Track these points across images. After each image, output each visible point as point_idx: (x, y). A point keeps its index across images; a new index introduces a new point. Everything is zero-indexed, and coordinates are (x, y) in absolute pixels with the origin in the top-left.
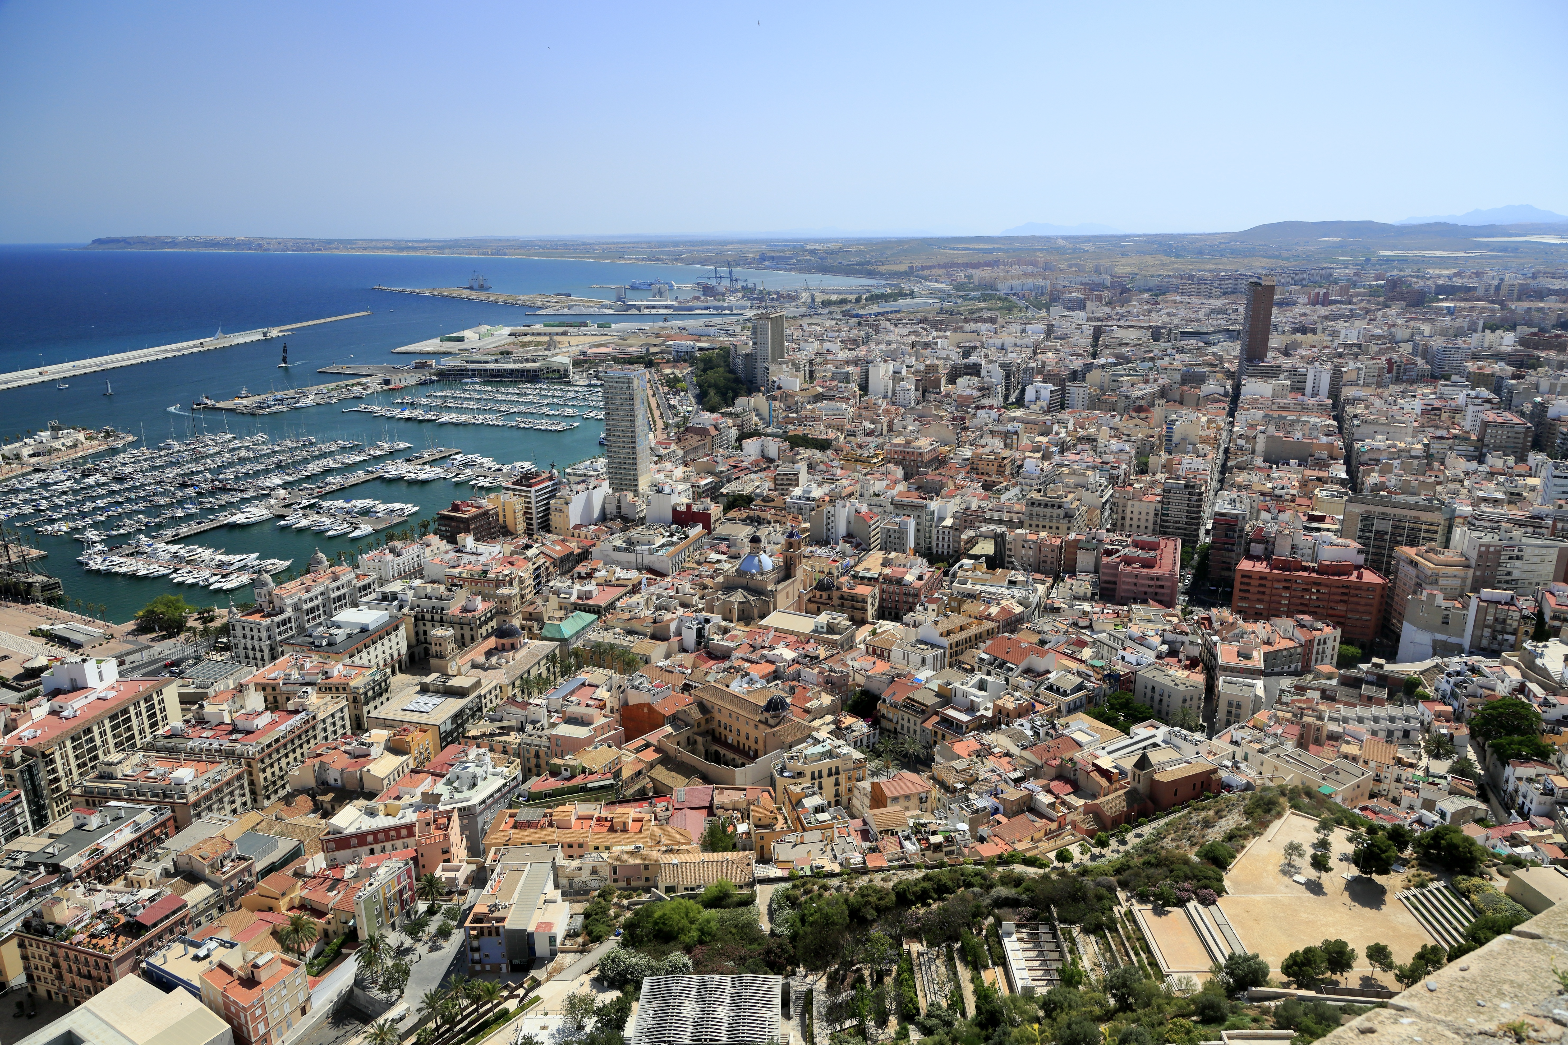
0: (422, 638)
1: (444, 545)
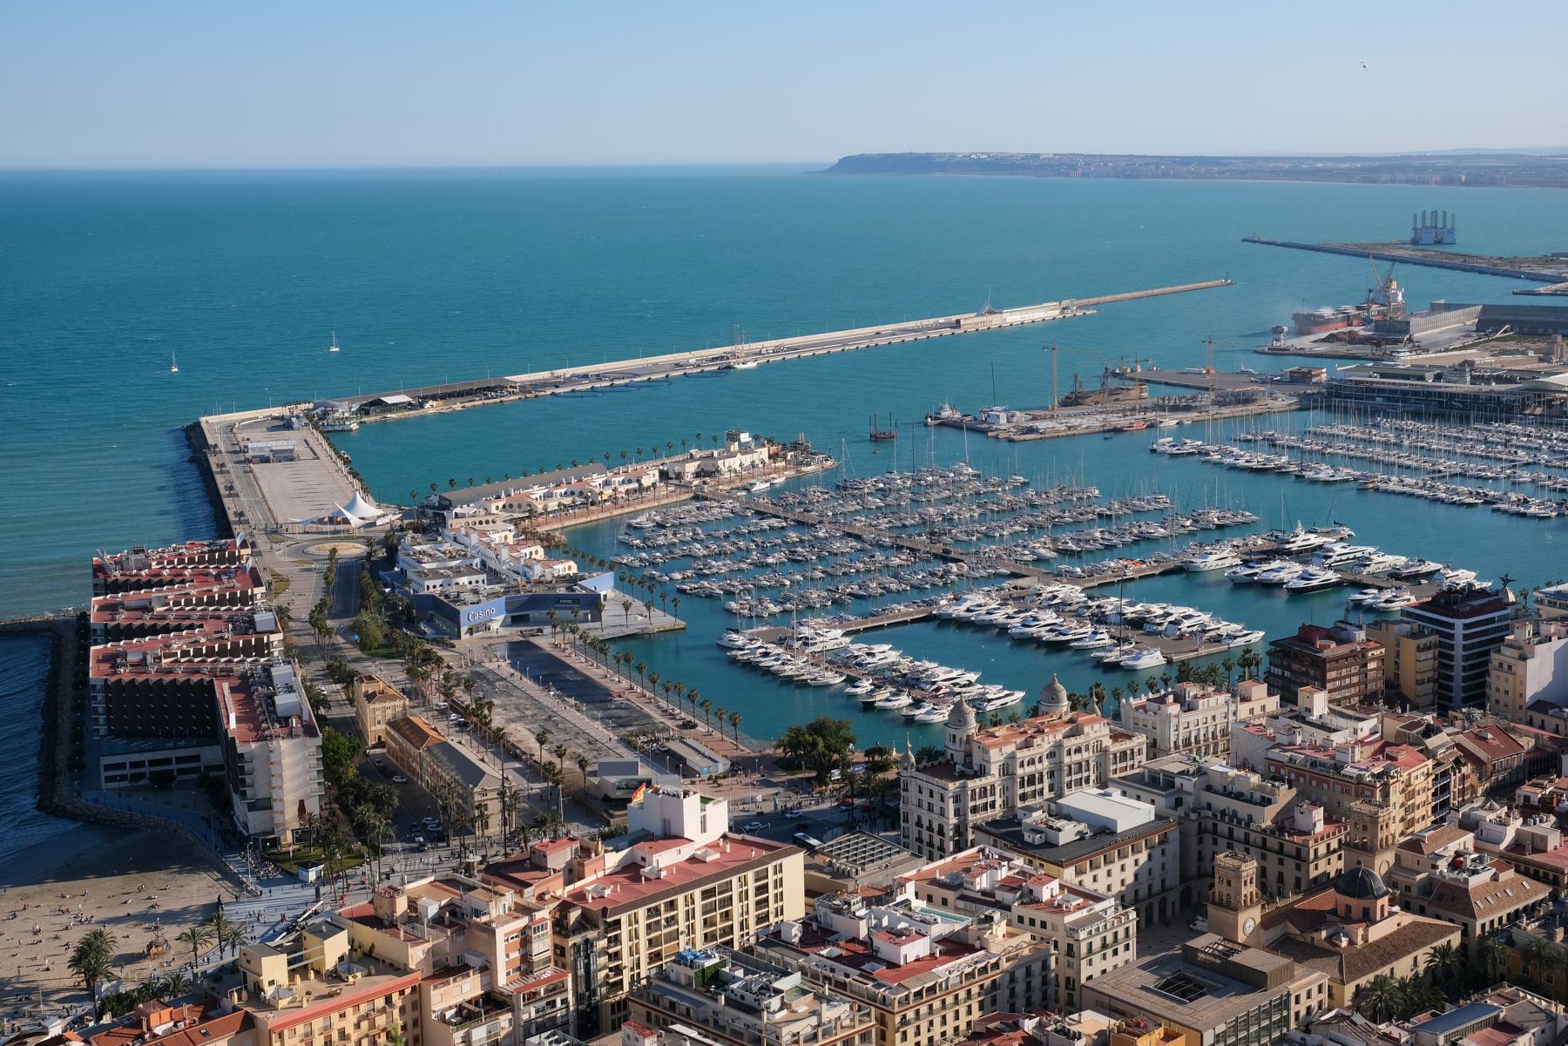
1: (1273, 703)
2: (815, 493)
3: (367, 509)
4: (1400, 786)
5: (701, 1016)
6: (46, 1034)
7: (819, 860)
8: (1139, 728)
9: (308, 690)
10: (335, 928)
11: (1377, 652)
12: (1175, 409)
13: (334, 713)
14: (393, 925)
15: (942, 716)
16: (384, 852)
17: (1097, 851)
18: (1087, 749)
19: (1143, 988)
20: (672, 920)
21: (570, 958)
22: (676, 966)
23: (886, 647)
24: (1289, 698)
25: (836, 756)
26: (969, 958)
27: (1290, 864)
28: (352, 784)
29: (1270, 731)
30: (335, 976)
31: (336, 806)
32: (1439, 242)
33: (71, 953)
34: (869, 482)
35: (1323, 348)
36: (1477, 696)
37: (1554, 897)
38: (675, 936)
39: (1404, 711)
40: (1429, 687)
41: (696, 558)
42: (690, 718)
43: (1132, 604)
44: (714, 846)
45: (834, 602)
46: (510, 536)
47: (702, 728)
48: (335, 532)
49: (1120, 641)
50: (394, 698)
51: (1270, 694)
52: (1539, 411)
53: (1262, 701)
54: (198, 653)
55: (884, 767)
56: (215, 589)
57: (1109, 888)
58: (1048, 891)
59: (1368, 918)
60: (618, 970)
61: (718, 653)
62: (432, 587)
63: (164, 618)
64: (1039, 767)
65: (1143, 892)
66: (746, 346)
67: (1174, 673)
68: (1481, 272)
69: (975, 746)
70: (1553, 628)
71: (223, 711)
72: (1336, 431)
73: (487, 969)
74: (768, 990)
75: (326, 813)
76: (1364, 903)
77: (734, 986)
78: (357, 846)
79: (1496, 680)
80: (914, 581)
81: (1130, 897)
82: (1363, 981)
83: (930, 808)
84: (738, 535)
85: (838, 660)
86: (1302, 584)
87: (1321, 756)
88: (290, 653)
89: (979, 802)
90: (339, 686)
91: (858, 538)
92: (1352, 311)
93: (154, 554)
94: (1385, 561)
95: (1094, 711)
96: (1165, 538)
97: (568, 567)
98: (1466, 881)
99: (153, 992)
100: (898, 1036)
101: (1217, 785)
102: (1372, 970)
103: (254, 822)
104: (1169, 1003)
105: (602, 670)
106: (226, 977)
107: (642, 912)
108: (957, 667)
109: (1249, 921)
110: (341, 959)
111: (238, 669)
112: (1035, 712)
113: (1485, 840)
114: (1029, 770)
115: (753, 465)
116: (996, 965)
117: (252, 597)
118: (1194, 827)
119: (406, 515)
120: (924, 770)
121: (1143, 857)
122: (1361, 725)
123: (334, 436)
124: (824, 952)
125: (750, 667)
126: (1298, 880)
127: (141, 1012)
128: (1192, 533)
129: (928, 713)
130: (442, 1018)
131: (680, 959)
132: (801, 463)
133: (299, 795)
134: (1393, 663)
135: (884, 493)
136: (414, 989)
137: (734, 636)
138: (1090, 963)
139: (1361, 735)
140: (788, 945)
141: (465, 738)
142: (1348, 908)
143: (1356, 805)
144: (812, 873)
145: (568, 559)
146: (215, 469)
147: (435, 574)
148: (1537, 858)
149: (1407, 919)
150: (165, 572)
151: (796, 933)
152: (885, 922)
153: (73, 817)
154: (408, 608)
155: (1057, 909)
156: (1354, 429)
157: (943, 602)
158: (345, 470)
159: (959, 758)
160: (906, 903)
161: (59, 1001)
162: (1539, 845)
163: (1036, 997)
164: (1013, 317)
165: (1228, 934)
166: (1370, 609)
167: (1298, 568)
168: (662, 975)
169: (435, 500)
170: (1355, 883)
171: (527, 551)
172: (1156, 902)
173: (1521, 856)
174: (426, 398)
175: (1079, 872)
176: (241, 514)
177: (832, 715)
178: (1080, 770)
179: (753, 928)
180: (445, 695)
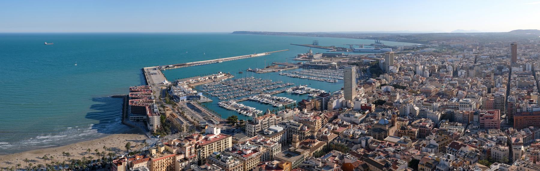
0: (291, 136)
2: (231, 81)
4: (317, 122)
5: (217, 163)
7: (234, 138)
8: (280, 116)
10: (163, 146)
12: (282, 68)
14: (171, 146)
15: (251, 115)
19: (283, 156)
20: (212, 147)
21: (197, 152)
22: (213, 155)
23: (242, 104)
24: (301, 110)
26: (257, 153)
27: (302, 135)
29: (299, 115)
30: (162, 153)
35: (302, 59)
38: (213, 149)
40: (320, 107)
44: (218, 135)
47: (215, 117)
49: (276, 103)
51: (298, 110)
53: (298, 111)
55: (242, 123)
58: (268, 142)
60: (204, 155)
61: (217, 105)
65: (281, 141)
66: (221, 59)
67: (284, 107)
73: (185, 154)
74: (227, 159)
77: (222, 158)
81: (280, 142)
83: (250, 129)
84: (220, 87)
85: (235, 106)
86: (301, 93)
87: (306, 119)
89: (257, 128)
91: (237, 88)
92: (306, 54)
97: (195, 92)
100: (247, 166)
101: (292, 124)
104: (287, 158)
107: (208, 146)
108: (252, 107)
109: (298, 144)
110: (163, 151)
112: (265, 114)
114: (265, 123)
115: (222, 77)
116: (261, 154)
121: (281, 135)
122: (311, 114)
125: (222, 107)
126: (304, 137)
128: (285, 86)
129: (249, 114)
131: (214, 153)
132: (229, 76)
134: (315, 104)
135: (241, 81)
136: (174, 156)
137: (220, 103)
139: (311, 115)
141: (181, 117)
143: (312, 126)
151: (231, 149)
155: (270, 144)
156: (307, 71)
157: (250, 97)
159: (254, 121)
160: (247, 144)
163: (267, 158)
164: (259, 55)
165: (295, 146)
166: (311, 97)
167: (301, 91)
168: (211, 156)
170: (312, 137)
171: (189, 89)
172: (283, 142)
175: (272, 139)
177: (234, 115)
178: (272, 123)
179: (224, 149)
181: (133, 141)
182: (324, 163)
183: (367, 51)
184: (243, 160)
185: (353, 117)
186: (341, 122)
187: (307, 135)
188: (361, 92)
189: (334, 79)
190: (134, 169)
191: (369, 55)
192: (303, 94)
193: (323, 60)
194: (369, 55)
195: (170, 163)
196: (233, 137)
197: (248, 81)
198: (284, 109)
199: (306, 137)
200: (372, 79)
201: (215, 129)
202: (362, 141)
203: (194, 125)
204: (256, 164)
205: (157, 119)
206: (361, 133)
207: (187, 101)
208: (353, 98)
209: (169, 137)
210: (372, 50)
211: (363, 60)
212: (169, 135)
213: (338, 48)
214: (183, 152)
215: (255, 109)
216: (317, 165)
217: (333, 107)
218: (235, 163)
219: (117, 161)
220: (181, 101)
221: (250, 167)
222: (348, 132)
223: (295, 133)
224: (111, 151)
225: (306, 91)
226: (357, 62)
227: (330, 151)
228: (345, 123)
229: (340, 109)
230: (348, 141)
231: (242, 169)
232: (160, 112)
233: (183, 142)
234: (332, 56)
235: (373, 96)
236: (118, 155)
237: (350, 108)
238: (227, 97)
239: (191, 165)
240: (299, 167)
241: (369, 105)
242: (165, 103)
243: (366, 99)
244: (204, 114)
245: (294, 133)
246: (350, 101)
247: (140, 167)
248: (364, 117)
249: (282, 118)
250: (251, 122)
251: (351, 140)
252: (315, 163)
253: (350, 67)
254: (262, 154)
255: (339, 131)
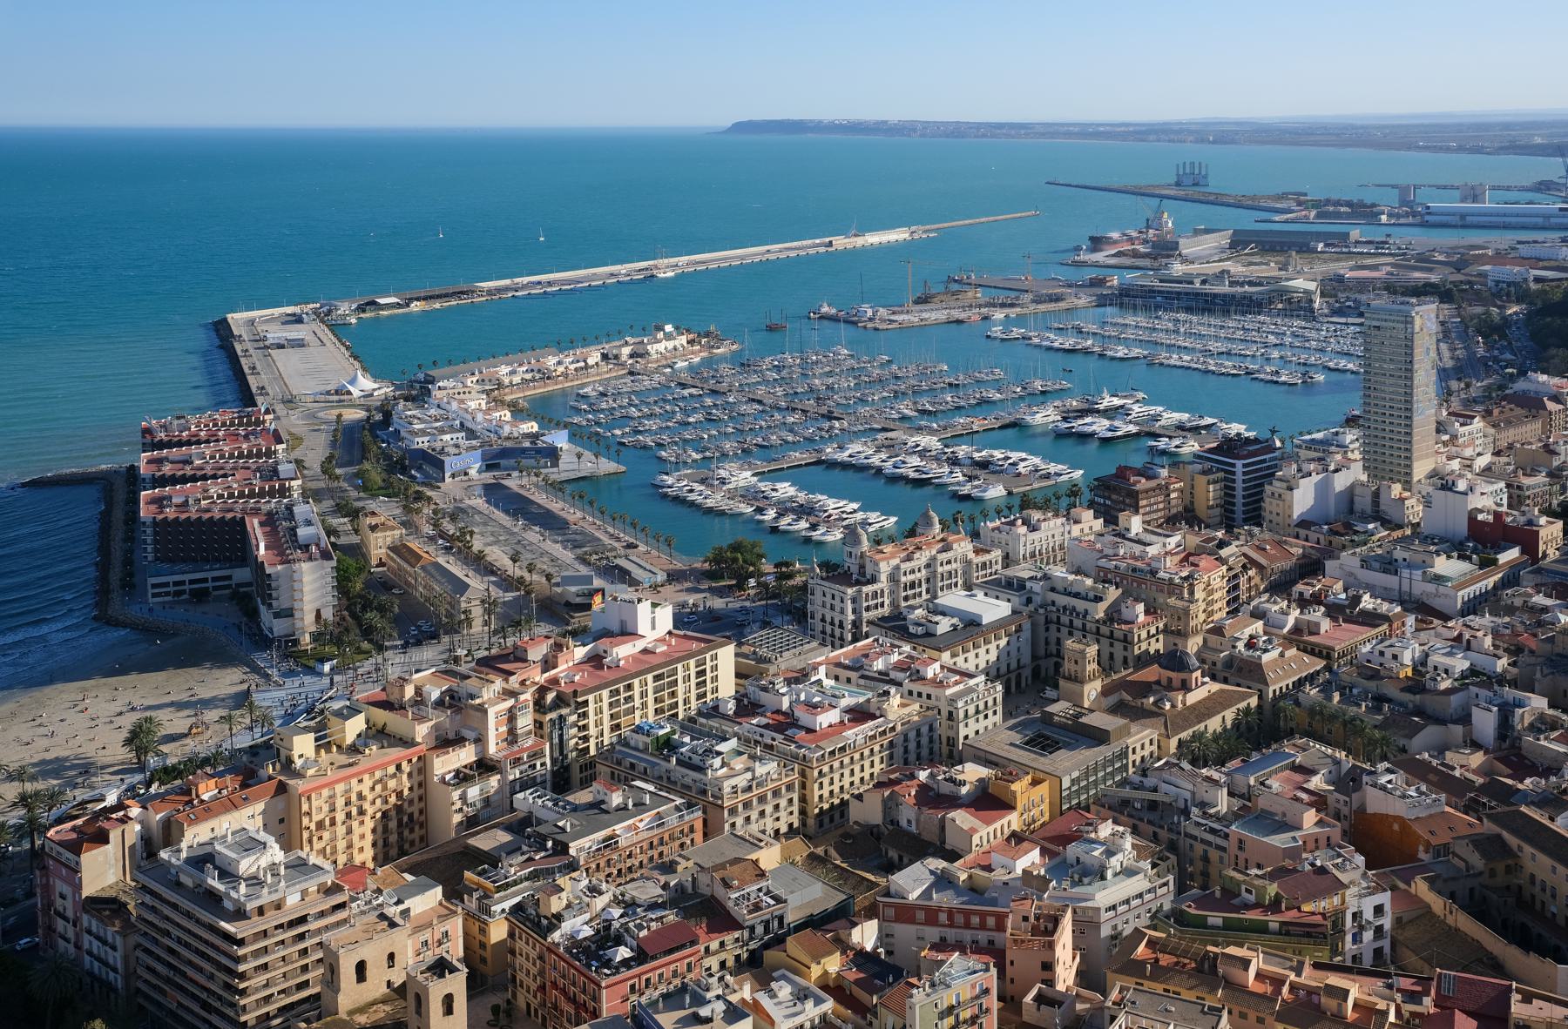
0: (1053, 649)
1: (1098, 524)
2: (725, 369)
3: (365, 383)
4: (1202, 586)
5: (656, 774)
6: (104, 800)
7: (746, 649)
8: (994, 544)
9: (323, 522)
10: (353, 711)
11: (1177, 486)
12: (1003, 305)
13: (343, 540)
14: (402, 707)
15: (837, 535)
16: (387, 649)
17: (967, 639)
18: (956, 561)
19: (1012, 744)
20: (629, 699)
21: (547, 729)
22: (635, 735)
23: (786, 484)
24: (1111, 520)
25: (752, 569)
26: (871, 724)
27: (1119, 646)
28: (360, 596)
29: (1098, 546)
30: (354, 749)
31: (346, 613)
32: (1196, 184)
33: (125, 734)
34: (767, 360)
35: (1113, 261)
36: (1255, 516)
37: (1328, 668)
38: (632, 710)
39: (1200, 529)
40: (1217, 511)
41: (632, 418)
42: (632, 540)
43: (979, 451)
44: (661, 640)
45: (744, 451)
46: (483, 403)
47: (642, 548)
48: (340, 401)
49: (971, 478)
50: (393, 528)
51: (1095, 518)
52: (1280, 306)
53: (1090, 523)
54: (231, 496)
55: (790, 576)
56: (244, 446)
57: (977, 666)
58: (932, 671)
59: (1185, 687)
60: (586, 739)
61: (652, 490)
62: (421, 443)
63: (202, 469)
64: (918, 575)
65: (1004, 669)
66: (666, 261)
67: (1016, 502)
68: (1229, 205)
69: (868, 560)
70: (1312, 466)
71: (254, 541)
72: (1127, 322)
73: (480, 740)
74: (710, 752)
75: (337, 619)
76: (1183, 675)
77: (683, 750)
78: (365, 645)
79: (1269, 505)
80: (806, 435)
81: (993, 672)
82: (1185, 735)
83: (832, 608)
84: (665, 401)
85: (749, 495)
86: (1109, 434)
87: (1139, 564)
88: (306, 494)
89: (871, 603)
90: (346, 520)
91: (760, 402)
92: (1134, 234)
93: (193, 420)
94: (1172, 417)
95: (959, 533)
96: (1001, 401)
97: (531, 427)
98: (1260, 657)
99: (196, 764)
100: (816, 786)
101: (1060, 587)
102: (1190, 727)
103: (279, 627)
104: (1033, 756)
105: (560, 505)
106: (262, 752)
107: (605, 693)
108: (843, 498)
109: (1092, 691)
110: (359, 735)
111: (265, 508)
112: (912, 533)
113: (1271, 627)
114: (911, 577)
115: (675, 349)
116: (893, 729)
117: (275, 452)
118: (1042, 619)
119: (397, 388)
120: (827, 579)
121: (1003, 642)
122: (1168, 540)
123: (338, 329)
124: (754, 722)
125: (679, 500)
126: (1125, 659)
127: (191, 783)
128: (1021, 397)
129: (823, 534)
130: (443, 780)
131: (638, 730)
132: (713, 347)
133: (317, 605)
134: (1189, 493)
135: (778, 369)
137: (665, 477)
138: (967, 725)
139: (1169, 548)
140: (725, 717)
141: (451, 560)
142: (1170, 680)
143: (1172, 601)
144: (740, 660)
145: (530, 420)
146: (239, 353)
147: (423, 433)
148: (1312, 639)
149: (1216, 687)
150: (202, 434)
151: (731, 707)
152: (803, 697)
153: (125, 626)
154: (402, 458)
155: (940, 684)
156: (1141, 320)
157: (828, 450)
158: (347, 354)
159: (854, 569)
160: (819, 682)
161: (112, 774)
162: (1314, 629)
163: (925, 752)
164: (873, 239)
165: (1077, 701)
166: (1164, 453)
167: (1106, 423)
168: (623, 741)
169: (421, 376)
170: (1174, 660)
171: (498, 414)
172: (1013, 676)
173: (1299, 637)
174: (411, 300)
175: (954, 655)
176: (263, 388)
177: (746, 537)
178: (950, 577)
179: (694, 704)
180: (434, 525)
181: (172, 704)
182: (1241, 796)
183: (1507, 220)
184: (795, 757)
185: (1418, 574)
186: (1343, 596)
187: (1144, 646)
188: (1471, 443)
189: (1302, 369)
190: (184, 855)
191: (1519, 243)
192: (1118, 437)
193: (1236, 268)
194: (1519, 243)
195: (399, 795)
196: (740, 644)
197: (818, 371)
198: (1016, 508)
199: (1139, 657)
200: (1543, 378)
201: (644, 609)
202: (1475, 710)
203: (528, 593)
204: (867, 777)
205: (315, 581)
206: (1466, 664)
207: (488, 477)
208: (1415, 471)
209: (394, 663)
210: (1547, 217)
211: (1487, 267)
212: (388, 654)
213: (1328, 202)
214: (467, 733)
215: (855, 506)
216: (1203, 805)
217: (1295, 517)
218: (753, 771)
219: (73, 829)
220: (453, 476)
221: (837, 790)
222: (1389, 653)
223: (1075, 632)
224: (33, 778)
225: (1136, 424)
226: (1444, 282)
227: (1278, 739)
228: (1367, 602)
229: (1338, 527)
230: (1389, 701)
231: (791, 801)
232: (333, 539)
233: (472, 684)
234: (1290, 246)
235: (1550, 474)
236: (81, 794)
237: (1400, 527)
238: (706, 449)
239: (513, 793)
240: (1098, 801)
241: (1522, 520)
242: (362, 494)
243: (1502, 485)
244: (578, 537)
245: (1071, 634)
246: (1397, 490)
247: (225, 836)
248: (1490, 582)
249: (1006, 557)
250: (837, 573)
251: (1407, 697)
252: (1193, 793)
253: (1402, 307)
254: (899, 728)
255: (1329, 643)
